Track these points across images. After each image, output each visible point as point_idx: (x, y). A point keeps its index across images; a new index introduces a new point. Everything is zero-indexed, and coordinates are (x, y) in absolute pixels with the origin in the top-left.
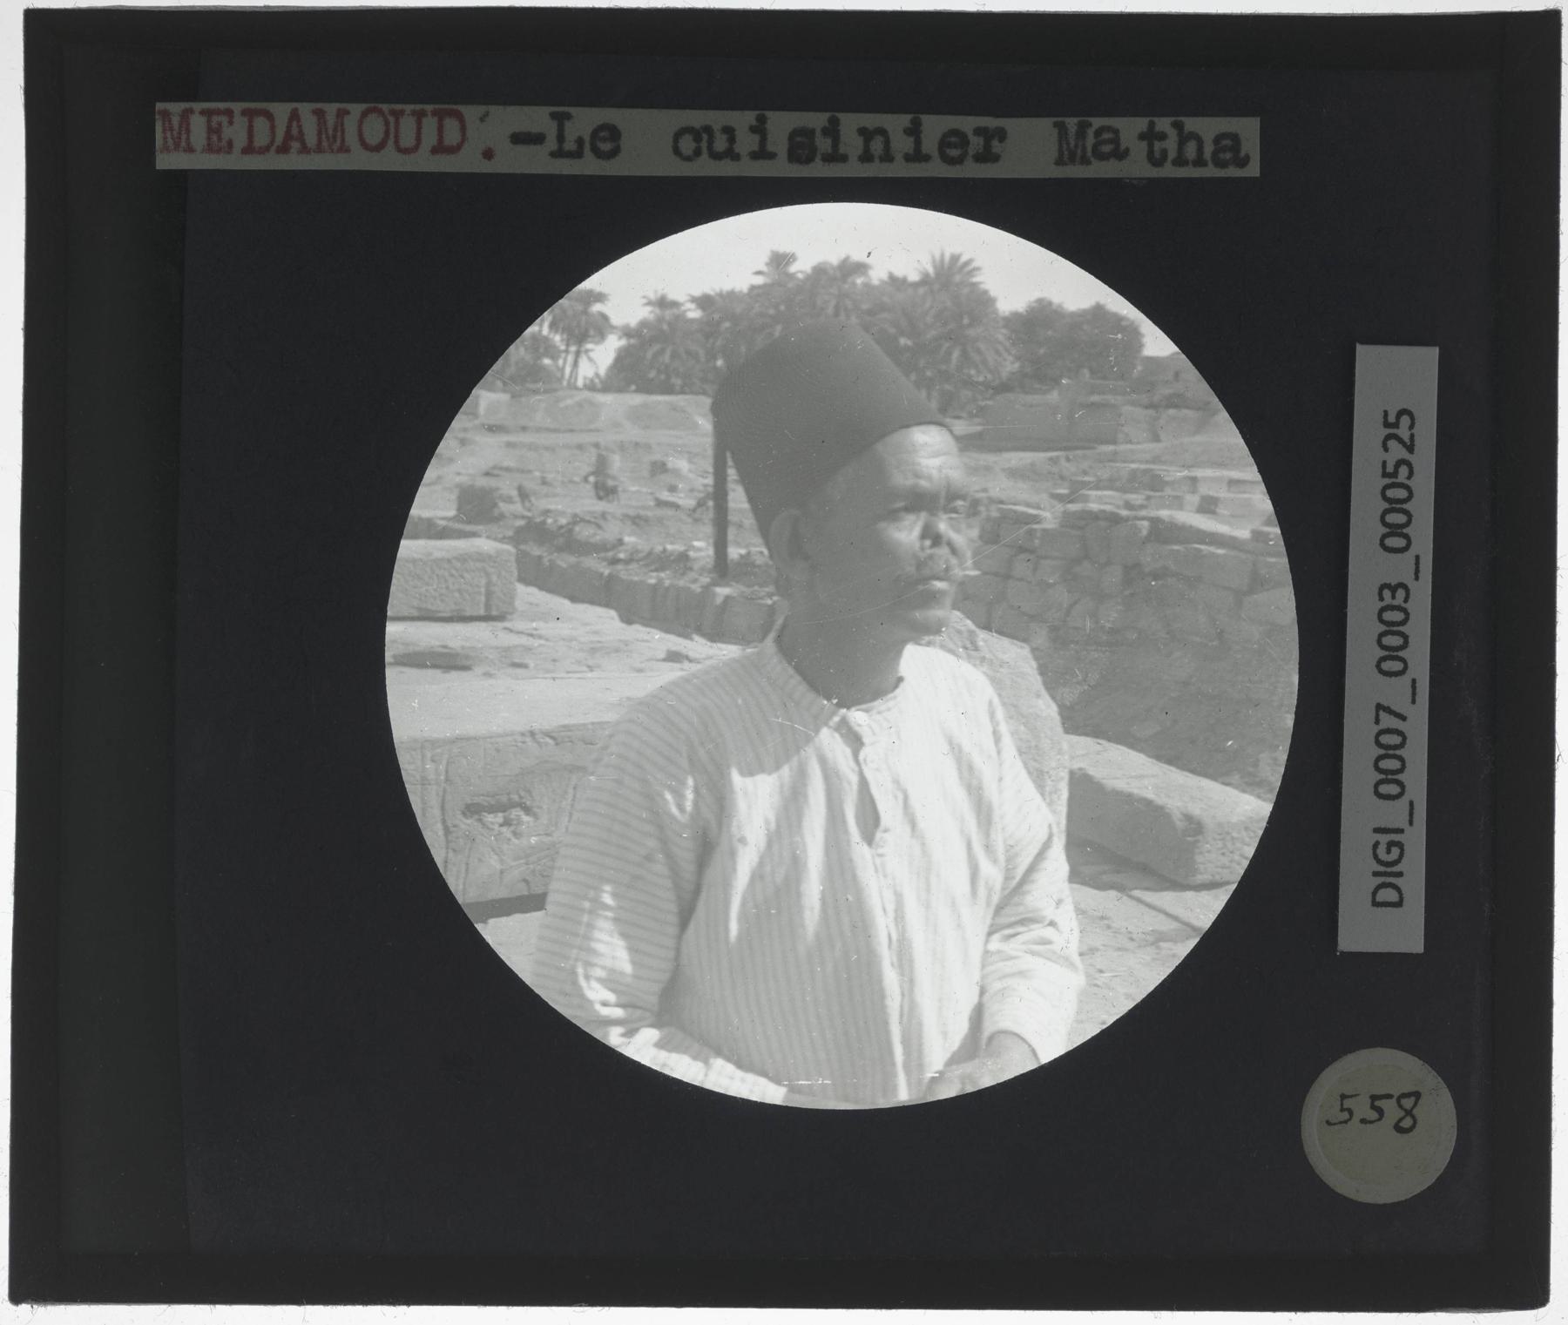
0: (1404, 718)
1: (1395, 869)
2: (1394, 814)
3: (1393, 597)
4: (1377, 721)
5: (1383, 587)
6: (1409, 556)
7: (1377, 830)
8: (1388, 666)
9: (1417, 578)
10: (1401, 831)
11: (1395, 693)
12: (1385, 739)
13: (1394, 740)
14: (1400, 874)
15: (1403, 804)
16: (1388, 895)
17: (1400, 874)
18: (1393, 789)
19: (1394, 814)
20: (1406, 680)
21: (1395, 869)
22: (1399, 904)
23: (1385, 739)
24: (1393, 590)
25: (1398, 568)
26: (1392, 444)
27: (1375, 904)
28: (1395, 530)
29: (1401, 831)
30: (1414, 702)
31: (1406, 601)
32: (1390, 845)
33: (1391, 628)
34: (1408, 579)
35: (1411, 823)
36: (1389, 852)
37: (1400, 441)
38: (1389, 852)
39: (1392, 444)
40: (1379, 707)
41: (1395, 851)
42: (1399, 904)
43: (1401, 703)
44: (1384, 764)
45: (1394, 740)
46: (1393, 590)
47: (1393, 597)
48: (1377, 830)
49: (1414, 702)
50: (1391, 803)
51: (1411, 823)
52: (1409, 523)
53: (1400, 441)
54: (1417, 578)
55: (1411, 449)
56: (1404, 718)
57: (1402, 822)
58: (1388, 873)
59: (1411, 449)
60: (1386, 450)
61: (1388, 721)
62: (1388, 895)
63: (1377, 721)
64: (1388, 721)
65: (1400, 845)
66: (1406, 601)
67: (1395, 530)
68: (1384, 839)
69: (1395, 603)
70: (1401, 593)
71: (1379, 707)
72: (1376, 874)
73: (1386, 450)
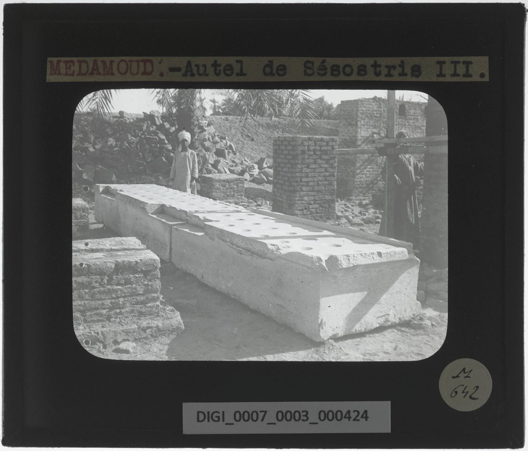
0: (262, 420)
1: (211, 420)
2: (229, 418)
3: (303, 416)
4: (261, 412)
5: (307, 412)
6: (318, 421)
7: (223, 412)
8: (280, 415)
9: (310, 423)
10: (223, 421)
11: (271, 417)
12: (255, 414)
13: (255, 417)
14: (209, 421)
15: (233, 421)
16: (201, 417)
17: (209, 421)
18: (238, 417)
19: (229, 418)
20: (275, 421)
21: (211, 420)
22: (198, 421)
23: (255, 414)
24: (306, 416)
25: (313, 417)
26: (356, 413)
27: (198, 412)
28: (326, 416)
29: (223, 421)
30: (268, 424)
31: (303, 420)
32: (219, 417)
33: (293, 416)
34: (310, 420)
35: (226, 424)
36: (216, 417)
37: (357, 416)
38: (216, 417)
39: (356, 413)
40: (266, 412)
41: (217, 419)
42: (198, 421)
43: (268, 419)
44: (246, 414)
45: (255, 417)
46: (306, 416)
47: (303, 416)
48: (223, 412)
49: (268, 424)
50: (233, 417)
51: (226, 424)
52: (330, 420)
53: (357, 416)
54: (310, 423)
55: (354, 420)
56: (262, 420)
57: (226, 421)
58: (209, 417)
59: (354, 420)
60: (354, 411)
61: (261, 415)
62: (201, 417)
63: (261, 412)
64: (261, 415)
65: (219, 420)
66: (303, 420)
67: (326, 416)
68: (221, 415)
69: (302, 416)
70: (305, 418)
71: (266, 412)
72: (208, 413)
73: (354, 411)
